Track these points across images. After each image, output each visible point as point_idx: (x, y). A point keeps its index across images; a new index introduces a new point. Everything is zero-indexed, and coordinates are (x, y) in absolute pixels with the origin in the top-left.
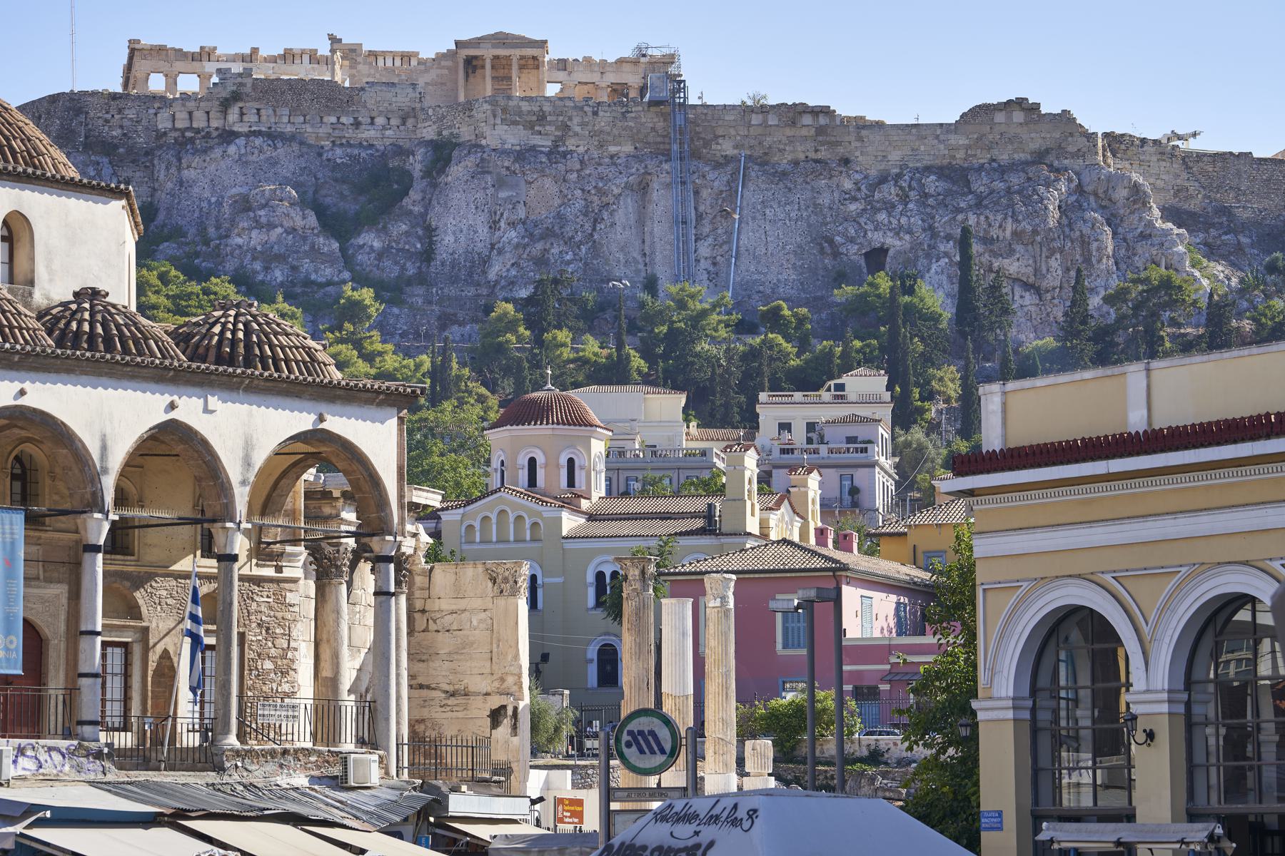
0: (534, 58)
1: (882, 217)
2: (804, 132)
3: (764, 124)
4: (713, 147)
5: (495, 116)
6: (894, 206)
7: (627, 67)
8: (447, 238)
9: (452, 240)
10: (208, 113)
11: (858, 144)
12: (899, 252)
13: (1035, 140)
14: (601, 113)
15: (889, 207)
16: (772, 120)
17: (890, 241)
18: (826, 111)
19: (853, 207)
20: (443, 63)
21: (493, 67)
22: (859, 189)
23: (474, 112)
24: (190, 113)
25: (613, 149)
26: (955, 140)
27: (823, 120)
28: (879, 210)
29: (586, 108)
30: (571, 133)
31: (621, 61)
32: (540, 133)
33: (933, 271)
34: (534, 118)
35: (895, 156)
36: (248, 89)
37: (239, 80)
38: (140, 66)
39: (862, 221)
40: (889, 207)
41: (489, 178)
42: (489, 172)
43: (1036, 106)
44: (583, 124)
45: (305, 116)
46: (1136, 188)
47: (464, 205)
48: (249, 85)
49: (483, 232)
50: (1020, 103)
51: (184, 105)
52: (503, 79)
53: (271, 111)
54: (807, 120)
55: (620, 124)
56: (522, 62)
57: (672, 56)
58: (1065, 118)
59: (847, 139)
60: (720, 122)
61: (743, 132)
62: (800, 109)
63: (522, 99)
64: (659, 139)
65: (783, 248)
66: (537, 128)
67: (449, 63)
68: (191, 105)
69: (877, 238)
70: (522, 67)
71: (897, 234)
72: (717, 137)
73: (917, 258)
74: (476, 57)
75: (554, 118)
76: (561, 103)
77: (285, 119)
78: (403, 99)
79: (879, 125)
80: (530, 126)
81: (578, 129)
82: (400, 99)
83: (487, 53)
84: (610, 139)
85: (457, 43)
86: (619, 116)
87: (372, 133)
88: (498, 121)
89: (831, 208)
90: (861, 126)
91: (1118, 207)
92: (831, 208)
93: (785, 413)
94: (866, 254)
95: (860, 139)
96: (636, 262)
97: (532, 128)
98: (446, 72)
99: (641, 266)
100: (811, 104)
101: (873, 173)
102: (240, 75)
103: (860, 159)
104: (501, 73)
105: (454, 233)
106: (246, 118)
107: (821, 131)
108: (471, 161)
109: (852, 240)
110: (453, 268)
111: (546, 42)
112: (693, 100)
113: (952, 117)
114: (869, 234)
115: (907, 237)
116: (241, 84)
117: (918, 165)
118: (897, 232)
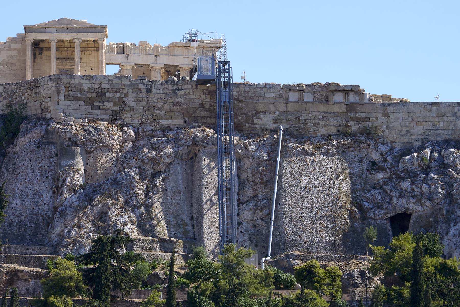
0: (95, 41)
1: (406, 184)
2: (336, 109)
3: (300, 101)
4: (255, 121)
5: (58, 93)
6: (416, 176)
7: (179, 51)
8: (15, 202)
9: (19, 203)
11: (385, 120)
12: (420, 217)
14: (154, 91)
15: (412, 176)
16: (308, 97)
19: (380, 176)
20: (14, 46)
21: (58, 50)
22: (385, 160)
23: (40, 90)
25: (165, 122)
27: (353, 98)
28: (404, 179)
29: (141, 86)
30: (127, 108)
31: (173, 46)
32: (99, 108)
33: (451, 233)
34: (94, 95)
35: (418, 130)
39: (388, 188)
40: (412, 176)
41: (53, 149)
42: (53, 143)
44: (137, 101)
47: (30, 172)
49: (47, 196)
54: (339, 97)
55: (171, 100)
56: (84, 45)
57: (219, 42)
59: (374, 115)
60: (261, 99)
61: (282, 108)
62: (332, 88)
63: (83, 78)
64: (206, 114)
65: (317, 213)
66: (96, 104)
67: (19, 46)
69: (401, 204)
70: (83, 50)
71: (419, 200)
72: (257, 113)
73: (436, 222)
74: (42, 41)
75: (111, 95)
76: (118, 81)
79: (403, 103)
80: (90, 102)
81: (133, 104)
83: (52, 37)
84: (162, 113)
85: (27, 29)
86: (171, 92)
88: (62, 97)
89: (360, 177)
90: (387, 103)
92: (360, 177)
94: (392, 219)
95: (386, 115)
96: (184, 223)
97: (92, 104)
98: (15, 53)
99: (189, 228)
100: (342, 83)
101: (398, 145)
103: (386, 133)
104: (65, 54)
105: (21, 197)
108: (37, 133)
109: (379, 206)
110: (20, 228)
111: (104, 27)
112: (236, 79)
114: (395, 200)
115: (428, 203)
117: (438, 139)
118: (419, 199)
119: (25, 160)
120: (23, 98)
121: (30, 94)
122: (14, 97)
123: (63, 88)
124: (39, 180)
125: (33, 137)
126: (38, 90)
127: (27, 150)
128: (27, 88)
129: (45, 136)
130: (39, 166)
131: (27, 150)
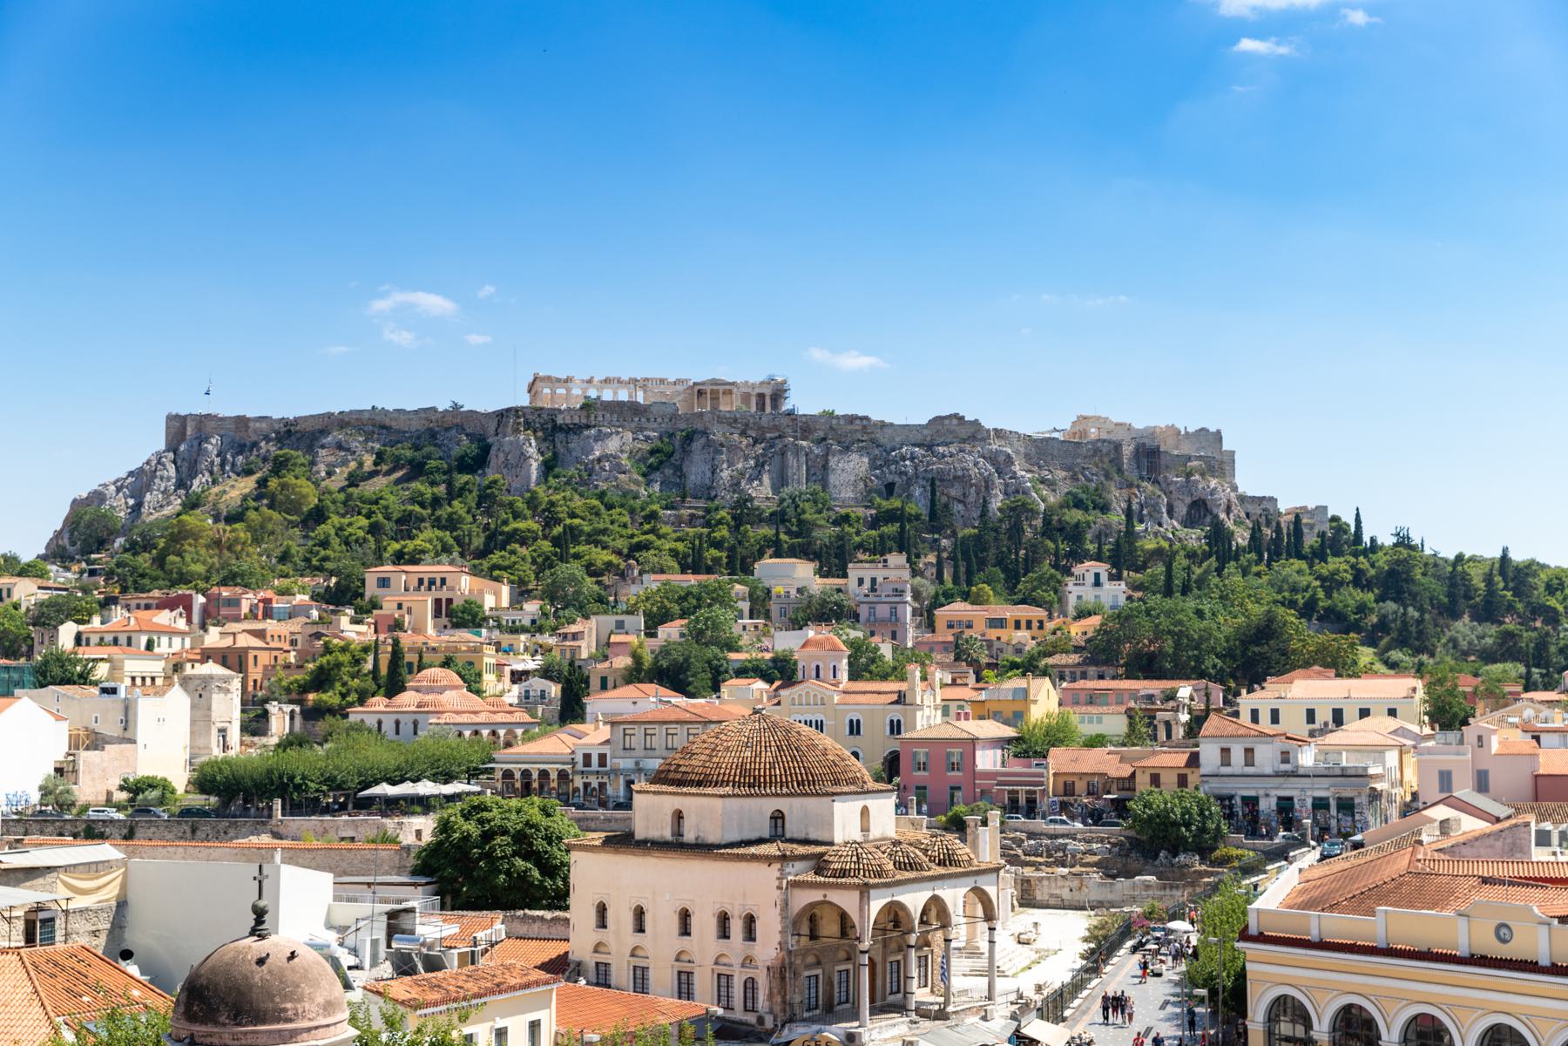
13: (964, 432)
17: (897, 479)
18: (866, 418)
26: (926, 432)
38: (538, 383)
43: (962, 418)
46: (1009, 456)
49: (709, 474)
50: (956, 416)
52: (715, 397)
58: (976, 423)
78: (669, 410)
79: (892, 425)
80: (730, 424)
83: (708, 388)
90: (883, 425)
91: (1002, 464)
93: (861, 573)
107: (864, 427)
108: (703, 440)
113: (925, 422)
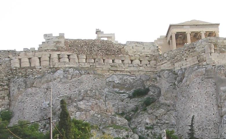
10: (40, 58)
23: (196, 49)
24: (30, 59)
36: (62, 45)
37: (57, 40)
45: (94, 59)
48: (63, 42)
51: (26, 55)
53: (75, 56)
68: (30, 55)
77: (84, 61)
82: (146, 50)
83: (188, 31)
87: (132, 69)
88: (213, 51)
102: (57, 37)
106: (61, 60)
116: (58, 42)
119: (195, 89)
120: (183, 57)
121: (188, 53)
122: (176, 58)
123: (213, 46)
124: (207, 100)
125: (198, 75)
126: (195, 50)
127: (195, 83)
128: (186, 50)
129: (206, 74)
130: (205, 92)
131: (195, 83)
